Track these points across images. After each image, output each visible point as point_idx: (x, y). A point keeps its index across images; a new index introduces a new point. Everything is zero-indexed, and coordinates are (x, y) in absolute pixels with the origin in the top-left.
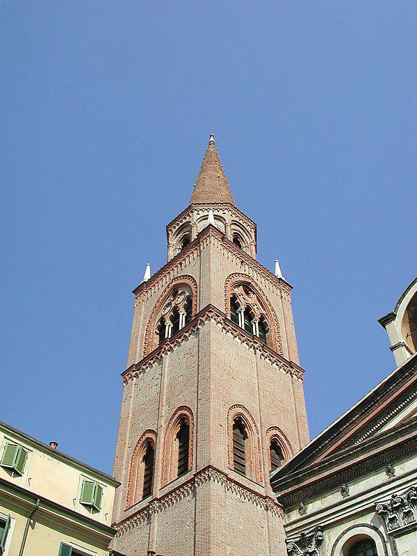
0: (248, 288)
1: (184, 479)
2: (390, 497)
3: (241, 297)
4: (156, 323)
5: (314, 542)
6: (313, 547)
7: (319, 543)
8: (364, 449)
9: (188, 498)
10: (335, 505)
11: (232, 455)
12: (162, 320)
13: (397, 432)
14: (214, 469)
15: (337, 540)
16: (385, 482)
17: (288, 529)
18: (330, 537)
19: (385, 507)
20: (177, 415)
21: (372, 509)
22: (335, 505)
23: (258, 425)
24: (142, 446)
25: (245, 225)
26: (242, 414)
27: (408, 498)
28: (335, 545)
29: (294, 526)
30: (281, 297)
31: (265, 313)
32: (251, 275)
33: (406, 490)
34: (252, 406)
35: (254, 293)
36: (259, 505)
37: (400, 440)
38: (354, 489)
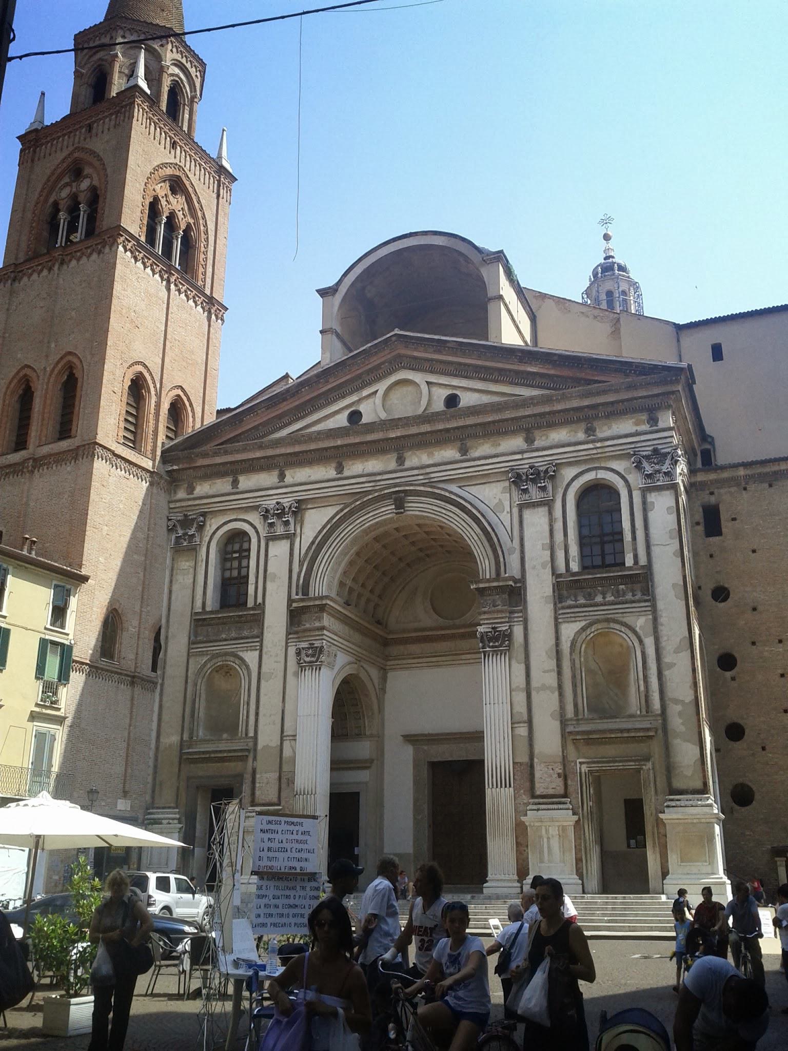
0: (177, 185)
1: (64, 445)
2: (274, 502)
3: (163, 202)
4: (48, 209)
5: (195, 525)
6: (193, 529)
7: (201, 528)
8: (261, 447)
9: (69, 469)
10: (223, 495)
11: (122, 425)
12: (56, 205)
13: (293, 439)
14: (101, 445)
15: (218, 529)
16: (274, 486)
17: (172, 506)
18: (212, 524)
19: (267, 511)
20: (62, 363)
21: (256, 508)
22: (223, 495)
23: (158, 386)
24: (19, 381)
25: (188, 65)
26: (141, 373)
27: (290, 508)
28: (214, 533)
29: (178, 505)
30: (218, 196)
31: (191, 221)
32: (182, 164)
33: (290, 499)
34: (154, 363)
35: (182, 191)
36: (144, 481)
37: (297, 449)
38: (246, 482)
